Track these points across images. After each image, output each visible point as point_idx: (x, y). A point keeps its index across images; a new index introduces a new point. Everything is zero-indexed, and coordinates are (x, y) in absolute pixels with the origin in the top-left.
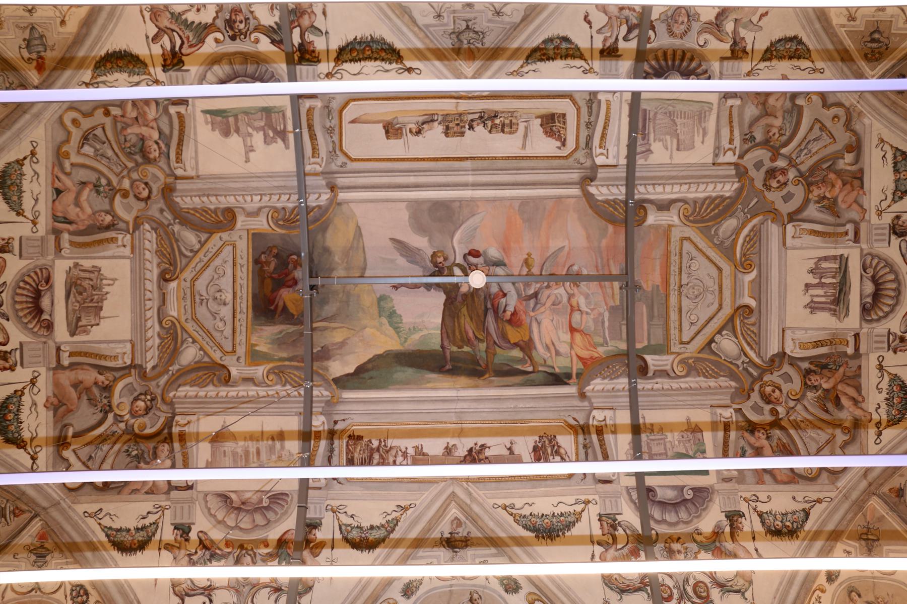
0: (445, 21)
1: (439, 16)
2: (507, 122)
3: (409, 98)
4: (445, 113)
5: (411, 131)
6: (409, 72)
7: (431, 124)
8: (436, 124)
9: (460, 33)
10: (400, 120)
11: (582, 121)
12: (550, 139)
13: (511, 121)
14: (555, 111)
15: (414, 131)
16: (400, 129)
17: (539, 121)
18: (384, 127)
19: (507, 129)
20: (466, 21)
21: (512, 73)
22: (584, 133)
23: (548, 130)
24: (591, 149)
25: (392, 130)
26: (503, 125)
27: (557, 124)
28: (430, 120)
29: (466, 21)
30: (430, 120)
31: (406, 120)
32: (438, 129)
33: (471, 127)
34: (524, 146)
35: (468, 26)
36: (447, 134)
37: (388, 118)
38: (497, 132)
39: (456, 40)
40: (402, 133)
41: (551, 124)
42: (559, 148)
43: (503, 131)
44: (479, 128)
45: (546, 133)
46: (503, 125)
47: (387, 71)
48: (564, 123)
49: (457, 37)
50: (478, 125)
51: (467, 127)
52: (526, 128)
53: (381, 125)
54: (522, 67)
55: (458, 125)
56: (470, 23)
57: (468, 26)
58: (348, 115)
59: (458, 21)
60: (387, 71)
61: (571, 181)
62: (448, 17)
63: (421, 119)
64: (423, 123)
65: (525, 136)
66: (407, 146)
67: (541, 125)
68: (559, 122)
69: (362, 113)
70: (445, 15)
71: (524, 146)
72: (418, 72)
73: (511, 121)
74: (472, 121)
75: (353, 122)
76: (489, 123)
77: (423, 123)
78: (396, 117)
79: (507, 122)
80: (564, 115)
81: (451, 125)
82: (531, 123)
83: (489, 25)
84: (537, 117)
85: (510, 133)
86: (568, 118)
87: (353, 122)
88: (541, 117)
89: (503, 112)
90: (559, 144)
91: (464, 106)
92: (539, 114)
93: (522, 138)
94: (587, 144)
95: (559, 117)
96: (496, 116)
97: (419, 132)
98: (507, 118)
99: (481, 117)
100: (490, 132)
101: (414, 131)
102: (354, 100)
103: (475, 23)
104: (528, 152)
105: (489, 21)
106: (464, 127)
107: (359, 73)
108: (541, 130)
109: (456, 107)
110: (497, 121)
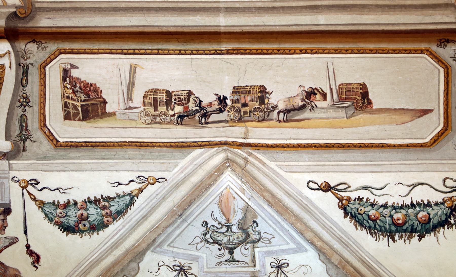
0: (268, 260)
1: (279, 267)
2: (162, 109)
3: (328, 146)
4: (266, 123)
5: (324, 96)
6: (328, 185)
7: (290, 107)
8: (281, 106)
9: (243, 242)
10: (342, 114)
11: (36, 108)
12: (89, 81)
13: (156, 109)
14: (84, 123)
15: (318, 97)
16: (342, 100)
17: (109, 109)
18: (370, 103)
19: (162, 97)
20: (233, 260)
21: (157, 180)
22: (32, 89)
23: (93, 95)
24: (19, 65)
25: (357, 98)
26: (168, 103)
27: (79, 104)
28: (290, 113)
29: (233, 260)
30: (290, 113)
31: (332, 114)
32: (278, 99)
33: (222, 100)
34: (133, 70)
35: (231, 253)
36: (263, 90)
37: (362, 117)
38: (178, 93)
39: (250, 230)
40: (340, 92)
41: (88, 104)
42: (73, 67)
43: (169, 94)
44: (208, 98)
45: (97, 90)
46: (168, 103)
47: (365, 188)
48: (66, 105)
49: (248, 235)
50: (211, 104)
51: (228, 102)
52: (130, 98)
53: (375, 107)
54: (140, 190)
55: (245, 105)
56: (228, 256)
57: (231, 253)
58: (433, 125)
59: (248, 260)
60: (365, 188)
61: (51, 15)
62: (263, 266)
63: (307, 114)
64: (303, 107)
65: (131, 86)
66: (330, 73)
67: (105, 102)
68: (75, 107)
69: (409, 124)
70: (269, 270)
71: (133, 70)
72: (312, 185)
73: (156, 109)
74: (220, 111)
75: (425, 112)
76: (192, 106)
77: (303, 107)
78: (349, 117)
79: (162, 109)
80: (67, 117)
81: (257, 104)
82: (122, 106)
83: (197, 254)
84: (113, 114)
85: (156, 91)
86: (61, 114)
87: (425, 112)
88: (105, 115)
89: (169, 123)
90: (74, 73)
91: (236, 133)
92: (109, 118)
93: (137, 82)
94: (26, 72)
95: (76, 115)
96: (181, 117)
97: (311, 94)
98: (161, 114)
99: (206, 115)
100: (190, 93)
101: (318, 97)
102: (422, 146)
103: (220, 256)
104: (125, 61)
105: (196, 259)
106: (233, 102)
107: (414, 186)
108: (104, 95)
109: (247, 132)
110: (179, 109)
